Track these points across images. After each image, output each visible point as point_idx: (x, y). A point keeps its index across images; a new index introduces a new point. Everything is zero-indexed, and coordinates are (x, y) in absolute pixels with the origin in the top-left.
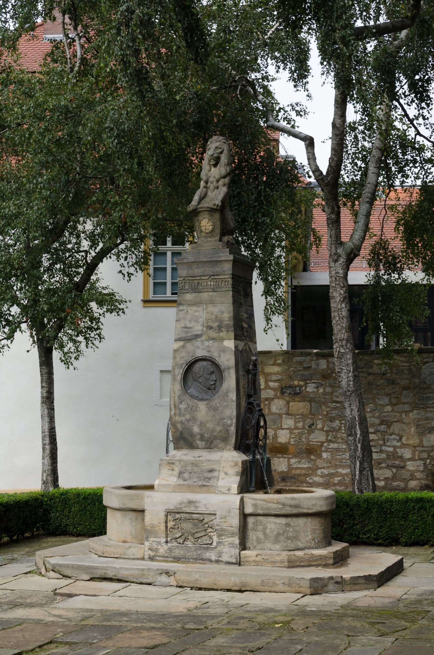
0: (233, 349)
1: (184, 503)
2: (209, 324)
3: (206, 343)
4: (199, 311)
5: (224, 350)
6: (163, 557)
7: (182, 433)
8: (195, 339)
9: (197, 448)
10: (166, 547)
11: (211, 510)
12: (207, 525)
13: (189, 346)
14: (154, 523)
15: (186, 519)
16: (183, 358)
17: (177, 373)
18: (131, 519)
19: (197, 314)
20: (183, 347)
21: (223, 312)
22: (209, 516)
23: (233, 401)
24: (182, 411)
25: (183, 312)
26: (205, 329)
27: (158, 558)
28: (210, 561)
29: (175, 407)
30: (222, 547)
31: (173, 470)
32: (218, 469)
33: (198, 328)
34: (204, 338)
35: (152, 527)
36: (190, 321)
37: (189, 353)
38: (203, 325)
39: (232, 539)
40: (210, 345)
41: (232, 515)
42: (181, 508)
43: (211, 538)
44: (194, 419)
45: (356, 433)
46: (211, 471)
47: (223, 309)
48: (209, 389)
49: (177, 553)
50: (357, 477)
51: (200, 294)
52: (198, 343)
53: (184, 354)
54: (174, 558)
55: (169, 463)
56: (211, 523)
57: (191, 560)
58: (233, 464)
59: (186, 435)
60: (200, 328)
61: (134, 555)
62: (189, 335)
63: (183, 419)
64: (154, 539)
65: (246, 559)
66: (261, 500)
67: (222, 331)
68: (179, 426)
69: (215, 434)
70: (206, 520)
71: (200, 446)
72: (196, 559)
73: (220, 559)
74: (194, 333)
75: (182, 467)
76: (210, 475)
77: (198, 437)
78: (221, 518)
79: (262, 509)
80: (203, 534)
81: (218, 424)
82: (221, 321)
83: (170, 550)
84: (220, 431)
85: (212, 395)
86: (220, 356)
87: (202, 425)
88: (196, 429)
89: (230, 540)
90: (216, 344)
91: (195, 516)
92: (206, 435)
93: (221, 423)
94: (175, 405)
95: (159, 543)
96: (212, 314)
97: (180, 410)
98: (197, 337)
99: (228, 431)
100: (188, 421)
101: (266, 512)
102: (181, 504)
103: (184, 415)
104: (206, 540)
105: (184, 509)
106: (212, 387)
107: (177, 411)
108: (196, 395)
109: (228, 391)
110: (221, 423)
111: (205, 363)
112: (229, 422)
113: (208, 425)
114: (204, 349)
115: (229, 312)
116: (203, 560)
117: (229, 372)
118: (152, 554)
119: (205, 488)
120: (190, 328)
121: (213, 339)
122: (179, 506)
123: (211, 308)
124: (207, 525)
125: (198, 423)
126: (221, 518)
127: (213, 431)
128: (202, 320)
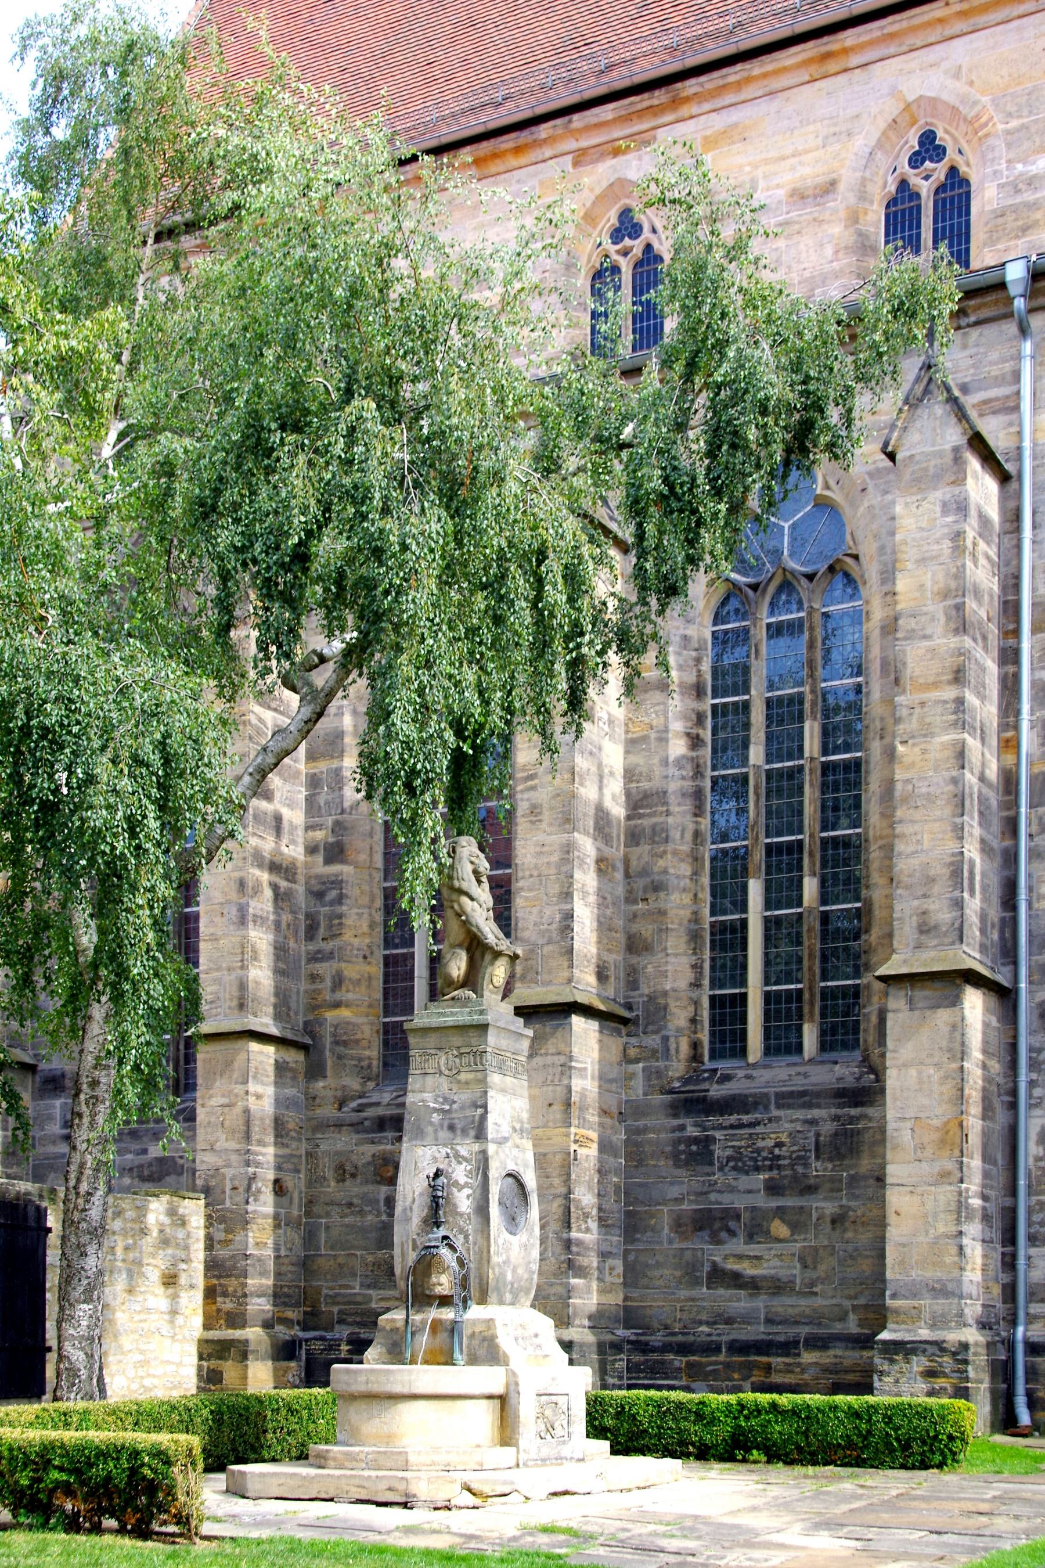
33: (506, 1130)
88: (509, 1277)
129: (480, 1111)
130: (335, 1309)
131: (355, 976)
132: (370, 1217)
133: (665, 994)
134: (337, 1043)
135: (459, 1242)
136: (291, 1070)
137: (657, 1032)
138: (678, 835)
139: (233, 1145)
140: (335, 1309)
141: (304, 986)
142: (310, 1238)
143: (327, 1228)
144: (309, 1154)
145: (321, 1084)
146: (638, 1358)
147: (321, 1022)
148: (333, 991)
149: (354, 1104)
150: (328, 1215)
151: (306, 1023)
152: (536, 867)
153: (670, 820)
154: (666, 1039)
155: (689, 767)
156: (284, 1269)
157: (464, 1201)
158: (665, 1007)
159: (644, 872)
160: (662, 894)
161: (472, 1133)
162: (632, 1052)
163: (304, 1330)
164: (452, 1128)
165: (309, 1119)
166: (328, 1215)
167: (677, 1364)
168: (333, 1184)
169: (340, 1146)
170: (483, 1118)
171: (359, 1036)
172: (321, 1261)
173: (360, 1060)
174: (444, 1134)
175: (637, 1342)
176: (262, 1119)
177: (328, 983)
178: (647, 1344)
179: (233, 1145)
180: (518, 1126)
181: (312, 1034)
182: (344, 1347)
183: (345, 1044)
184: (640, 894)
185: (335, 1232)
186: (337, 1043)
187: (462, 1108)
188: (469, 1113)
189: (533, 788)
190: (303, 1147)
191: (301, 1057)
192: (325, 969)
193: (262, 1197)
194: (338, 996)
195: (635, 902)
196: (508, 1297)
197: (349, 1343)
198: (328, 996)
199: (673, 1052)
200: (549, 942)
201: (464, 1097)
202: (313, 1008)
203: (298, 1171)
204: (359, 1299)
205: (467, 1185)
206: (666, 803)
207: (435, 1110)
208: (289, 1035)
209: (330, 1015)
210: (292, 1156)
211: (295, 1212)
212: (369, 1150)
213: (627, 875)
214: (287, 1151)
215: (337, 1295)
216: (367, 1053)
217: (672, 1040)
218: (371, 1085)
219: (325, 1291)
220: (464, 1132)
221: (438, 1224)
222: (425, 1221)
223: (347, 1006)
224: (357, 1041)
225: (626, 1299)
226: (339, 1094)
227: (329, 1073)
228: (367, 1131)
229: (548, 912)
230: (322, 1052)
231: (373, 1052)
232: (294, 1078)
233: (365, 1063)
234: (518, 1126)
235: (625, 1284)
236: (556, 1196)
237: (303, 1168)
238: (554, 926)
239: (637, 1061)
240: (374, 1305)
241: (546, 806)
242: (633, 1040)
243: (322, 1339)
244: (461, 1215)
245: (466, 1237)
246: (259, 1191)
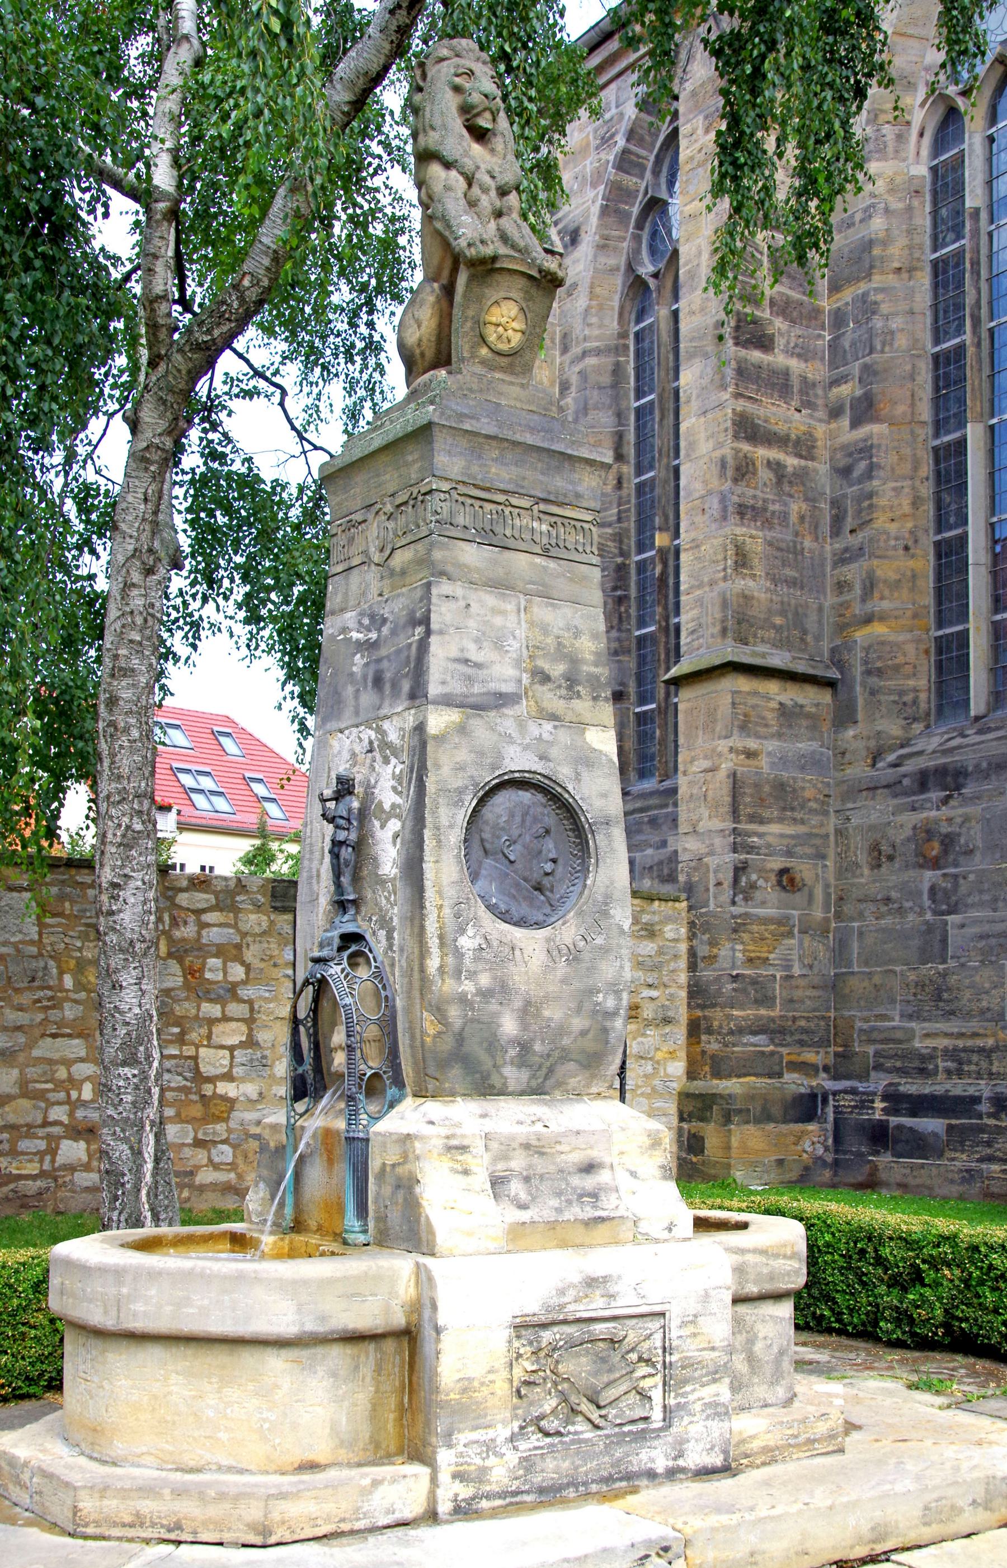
0: (616, 759)
1: (572, 1285)
2: (542, 664)
3: (534, 729)
4: (503, 613)
5: (586, 759)
6: (503, 1495)
7: (460, 1039)
8: (498, 707)
9: (502, 1093)
10: (512, 1458)
11: (653, 1299)
12: (634, 1356)
13: (480, 729)
14: (470, 1374)
15: (572, 1344)
16: (460, 768)
17: (444, 821)
18: (334, 1375)
19: (498, 621)
20: (462, 729)
21: (577, 635)
22: (640, 1323)
23: (622, 932)
24: (467, 961)
25: (452, 605)
26: (526, 679)
27: (485, 1504)
28: (651, 1475)
29: (442, 945)
30: (686, 1419)
31: (466, 1172)
32: (607, 1160)
33: (504, 673)
34: (523, 707)
35: (464, 1391)
36: (477, 641)
37: (481, 754)
38: (518, 663)
39: (712, 1389)
40: (546, 736)
41: (713, 1306)
42: (562, 1307)
43: (645, 1397)
44: (501, 990)
45: (148, 1057)
46: (589, 1168)
47: (578, 622)
48: (539, 888)
49: (552, 1469)
50: (148, 1178)
51: (508, 554)
52: (507, 721)
53: (463, 755)
54: (541, 1491)
55: (449, 1148)
56: (646, 1345)
57: (594, 1488)
58: (648, 1142)
59: (475, 1048)
60: (511, 672)
61: (390, 1511)
62: (477, 689)
63: (468, 987)
64: (476, 1435)
65: (742, 1449)
66: (755, 1251)
67: (579, 696)
68: (454, 1013)
69: (566, 1041)
70: (632, 1338)
71: (512, 1086)
72: (608, 1480)
73: (681, 1462)
74: (493, 686)
75: (495, 1160)
76: (589, 1182)
77: (512, 1052)
78: (683, 1324)
79: (758, 1279)
80: (624, 1388)
81: (579, 1010)
82: (574, 661)
83: (527, 1463)
84: (583, 1033)
85: (547, 910)
86: (578, 778)
87: (528, 1011)
88: (509, 1026)
89: (707, 1393)
90: (564, 737)
91: (599, 1327)
92: (537, 1047)
93: (587, 1006)
94: (441, 937)
95: (489, 1447)
96: (545, 629)
97: (459, 954)
98: (502, 700)
99: (605, 1031)
100: (485, 994)
101: (768, 1287)
102: (562, 1292)
103: (472, 975)
104: (631, 1407)
105: (571, 1308)
106: (546, 882)
107: (450, 960)
108: (503, 907)
109: (608, 899)
110: (587, 1006)
111: (526, 796)
112: (610, 1003)
113: (546, 1013)
114: (526, 748)
115: (595, 636)
116: (629, 1477)
117: (609, 836)
118: (465, 1492)
119: (603, 1228)
120: (478, 666)
121: (553, 717)
122: (555, 1301)
123: (542, 612)
124: (634, 1356)
125: (518, 1004)
126: (683, 1324)
127: (562, 1031)
128: (516, 645)
129: (419, 630)
130: (871, 1050)
131: (893, 576)
132: (911, 917)
134: (868, 672)
136: (809, 716)
139: (717, 824)
140: (871, 1050)
141: (830, 600)
142: (840, 952)
143: (861, 934)
144: (839, 832)
145: (851, 733)
147: (849, 646)
148: (863, 601)
149: (891, 758)
150: (861, 916)
151: (833, 651)
156: (798, 994)
161: (406, 686)
163: (835, 1078)
164: (378, 681)
165: (840, 783)
166: (861, 916)
168: (866, 871)
169: (874, 818)
170: (423, 646)
171: (900, 660)
172: (853, 982)
173: (901, 693)
174: (368, 698)
176: (756, 786)
177: (858, 590)
179: (717, 824)
180: (558, 670)
181: (839, 664)
182: (879, 1105)
183: (880, 672)
185: (869, 940)
186: (868, 672)
187: (394, 632)
188: (402, 641)
190: (832, 822)
191: (826, 697)
192: (853, 572)
193: (758, 895)
194: (869, 607)
196: (513, 1075)
197: (885, 1098)
198: (857, 609)
201: (395, 608)
202: (841, 628)
203: (824, 857)
204: (899, 1035)
205: (394, 811)
208: (801, 667)
209: (861, 635)
210: (810, 835)
211: (818, 914)
212: (910, 819)
214: (802, 829)
215: (873, 1029)
216: (911, 683)
218: (918, 727)
219: (859, 1024)
223: (882, 619)
224: (897, 668)
226: (872, 743)
227: (860, 716)
228: (906, 794)
230: (851, 688)
231: (921, 682)
232: (813, 728)
233: (908, 698)
234: (558, 670)
237: (831, 853)
240: (917, 1044)
243: (853, 1091)
245: (390, 937)
246: (753, 886)
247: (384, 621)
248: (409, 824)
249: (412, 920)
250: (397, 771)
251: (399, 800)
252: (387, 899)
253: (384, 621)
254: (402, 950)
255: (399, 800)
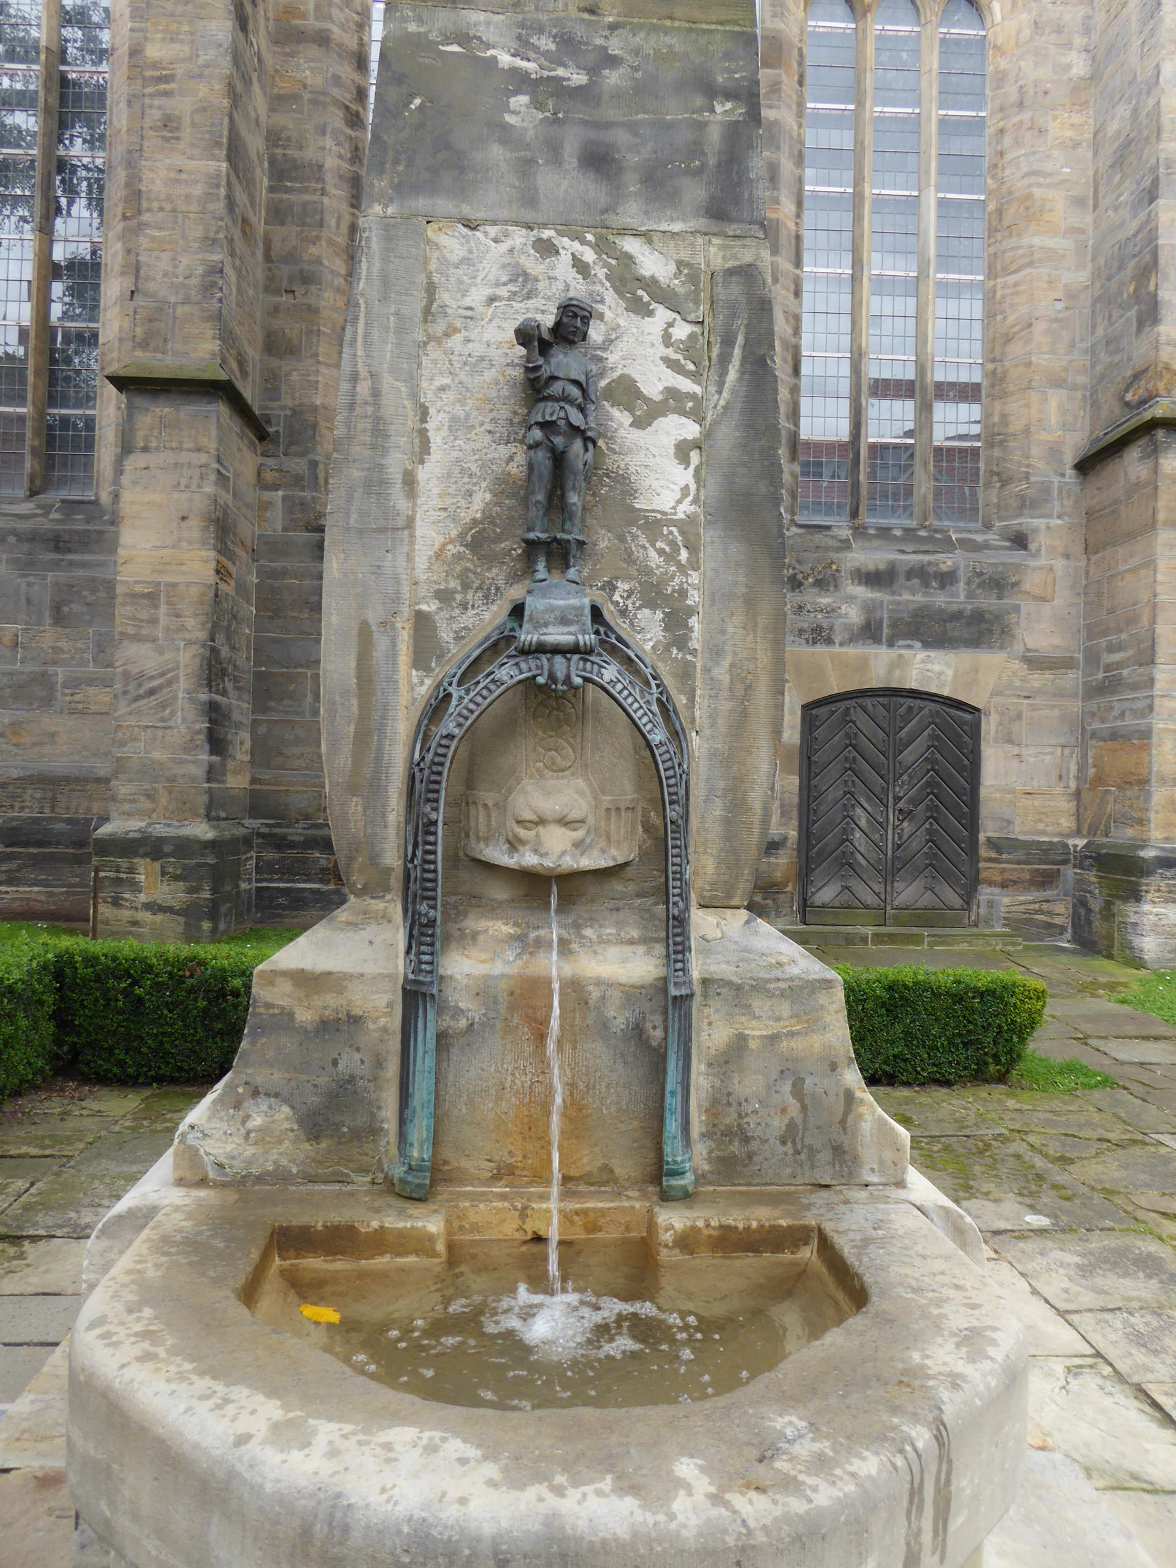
133: (315, 409)
135: (647, 632)
137: (302, 455)
138: (333, 222)
146: (271, 855)
152: (169, 198)
153: (326, 200)
154: (314, 464)
155: (347, 146)
157: (661, 467)
158: (314, 426)
159: (291, 257)
160: (313, 288)
161: (696, 192)
162: (269, 477)
164: (599, 161)
167: (323, 863)
174: (563, 184)
175: (271, 835)
178: (283, 837)
184: (285, 284)
187: (642, 91)
189: (167, 94)
195: (277, 292)
199: (321, 482)
200: (187, 301)
205: (673, 401)
206: (321, 180)
207: (520, 81)
213: (268, 258)
217: (321, 466)
220: (658, 186)
221: (558, 553)
222: (478, 541)
225: (254, 781)
229: (185, 260)
235: (252, 763)
236: (189, 643)
238: (193, 281)
239: (276, 487)
241: (187, 120)
242: (270, 462)
244: (653, 525)
245: (676, 622)
247: (613, 61)
248: (728, 435)
249: (750, 602)
250: (682, 331)
251: (686, 385)
252: (670, 557)
253: (613, 61)
254: (716, 652)
255: (686, 385)
